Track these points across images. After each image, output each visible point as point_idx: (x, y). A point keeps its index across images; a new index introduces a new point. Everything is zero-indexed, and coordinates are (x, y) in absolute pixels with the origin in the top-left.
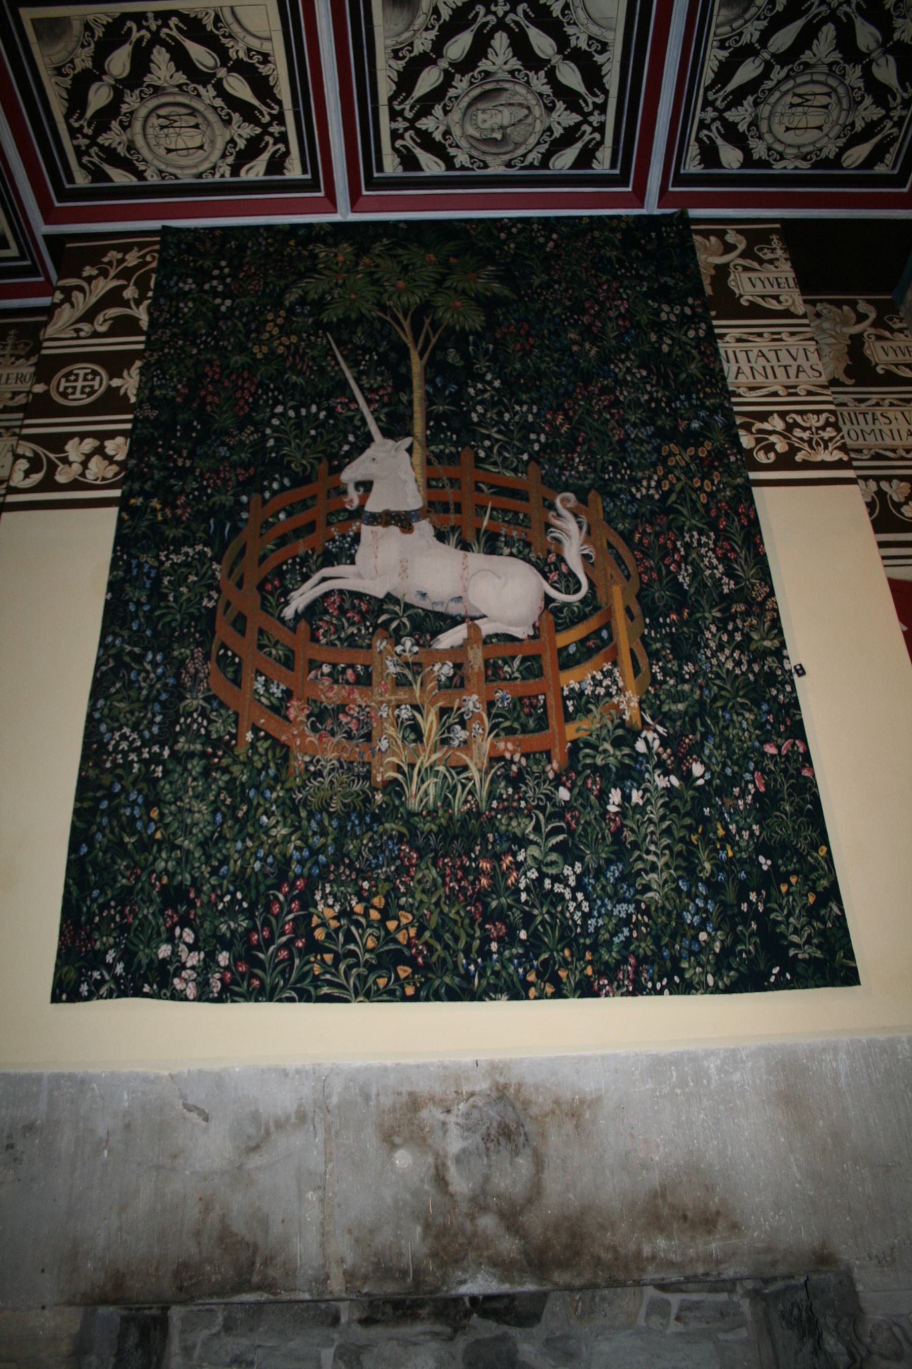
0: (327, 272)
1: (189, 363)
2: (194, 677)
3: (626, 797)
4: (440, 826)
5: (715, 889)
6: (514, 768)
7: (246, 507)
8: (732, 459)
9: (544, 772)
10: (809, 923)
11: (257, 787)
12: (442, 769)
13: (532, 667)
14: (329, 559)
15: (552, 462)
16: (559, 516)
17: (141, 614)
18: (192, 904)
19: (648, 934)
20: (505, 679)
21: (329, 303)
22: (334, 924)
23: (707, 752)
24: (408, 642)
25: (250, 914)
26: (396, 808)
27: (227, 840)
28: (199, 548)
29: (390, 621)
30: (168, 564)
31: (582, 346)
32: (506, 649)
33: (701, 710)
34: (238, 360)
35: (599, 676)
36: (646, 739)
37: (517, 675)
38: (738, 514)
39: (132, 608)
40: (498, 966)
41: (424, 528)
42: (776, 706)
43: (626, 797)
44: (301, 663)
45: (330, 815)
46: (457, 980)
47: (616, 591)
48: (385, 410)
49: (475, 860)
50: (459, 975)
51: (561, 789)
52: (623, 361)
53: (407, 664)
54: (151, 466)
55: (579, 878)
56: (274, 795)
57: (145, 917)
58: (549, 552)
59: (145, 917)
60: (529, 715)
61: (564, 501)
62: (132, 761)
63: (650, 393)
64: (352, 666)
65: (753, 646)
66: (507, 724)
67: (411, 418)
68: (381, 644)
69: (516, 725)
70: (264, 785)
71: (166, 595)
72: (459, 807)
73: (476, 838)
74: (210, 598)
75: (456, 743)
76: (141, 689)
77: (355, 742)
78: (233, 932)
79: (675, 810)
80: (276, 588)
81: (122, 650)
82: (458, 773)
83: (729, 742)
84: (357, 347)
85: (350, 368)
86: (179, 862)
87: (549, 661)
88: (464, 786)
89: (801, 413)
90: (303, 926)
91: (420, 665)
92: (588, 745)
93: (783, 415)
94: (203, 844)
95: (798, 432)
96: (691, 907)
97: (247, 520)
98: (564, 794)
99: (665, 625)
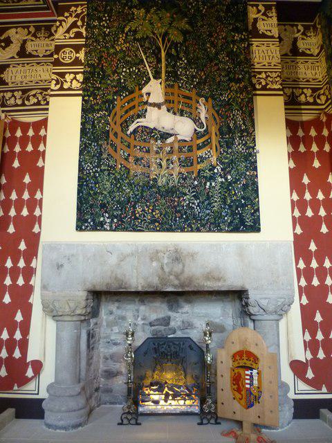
1: (98, 51)
3: (211, 184)
5: (230, 206)
7: (116, 100)
11: (122, 179)
14: (139, 116)
15: (199, 88)
24: (159, 141)
25: (121, 210)
29: (154, 135)
32: (184, 144)
34: (112, 51)
41: (164, 108)
43: (211, 184)
44: (132, 146)
47: (214, 127)
61: (202, 100)
68: (152, 142)
72: (171, 185)
80: (125, 125)
87: (195, 148)
89: (271, 72)
93: (266, 72)
95: (269, 79)
98: (196, 183)
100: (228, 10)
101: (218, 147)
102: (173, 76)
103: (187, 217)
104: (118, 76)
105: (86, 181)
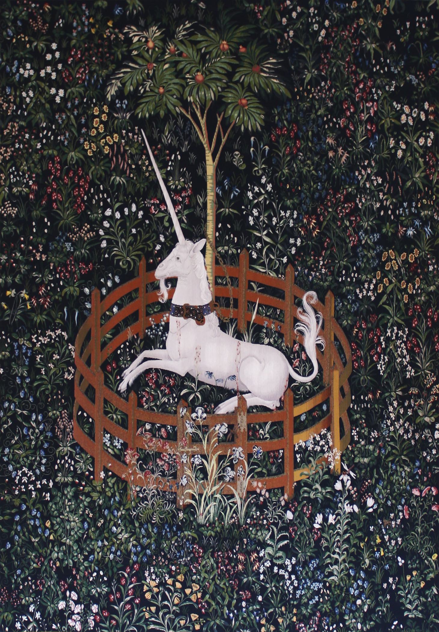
0: (140, 61)
3: (325, 519)
4: (216, 532)
6: (262, 499)
7: (88, 298)
8: (431, 268)
9: (279, 501)
10: (418, 598)
11: (109, 508)
12: (218, 496)
17: (25, 386)
18: (74, 578)
19: (329, 600)
20: (260, 439)
21: (142, 97)
22: (156, 590)
23: (377, 491)
24: (200, 410)
25: (108, 584)
26: (191, 522)
27: (92, 540)
28: (59, 332)
29: (188, 394)
30: (38, 345)
31: (336, 151)
33: (378, 463)
35: (318, 438)
36: (342, 481)
37: (267, 436)
38: (426, 317)
39: (18, 381)
40: (245, 615)
41: (212, 319)
42: (424, 464)
43: (325, 519)
44: (132, 423)
45: (153, 525)
46: (223, 621)
47: (336, 374)
48: (186, 212)
49: (235, 554)
50: (224, 619)
51: (288, 512)
52: (365, 168)
54: (17, 261)
55: (294, 566)
56: (120, 513)
57: (49, 586)
58: (295, 343)
59: (49, 586)
60: (273, 464)
62: (31, 490)
63: (381, 201)
64: (164, 426)
65: (418, 421)
66: (259, 470)
67: (206, 221)
68: (183, 411)
69: (264, 471)
70: (113, 507)
71: (40, 370)
72: (228, 520)
73: (237, 540)
74: (69, 372)
75: (227, 479)
76: (31, 440)
77: (167, 478)
78: (100, 594)
79: (353, 527)
80: (114, 368)
81: (16, 412)
82: (228, 499)
83: (392, 484)
84: (165, 147)
85: (160, 169)
86: (65, 553)
87: (288, 426)
88: (231, 507)
90: (139, 591)
91: (207, 426)
92: (306, 484)
94: (77, 542)
96: (355, 585)
97: (90, 309)
98: (289, 515)
99: (364, 401)
100: (387, 34)
102: (234, 231)
103: (266, 599)
104: (91, 230)
105: (21, 513)
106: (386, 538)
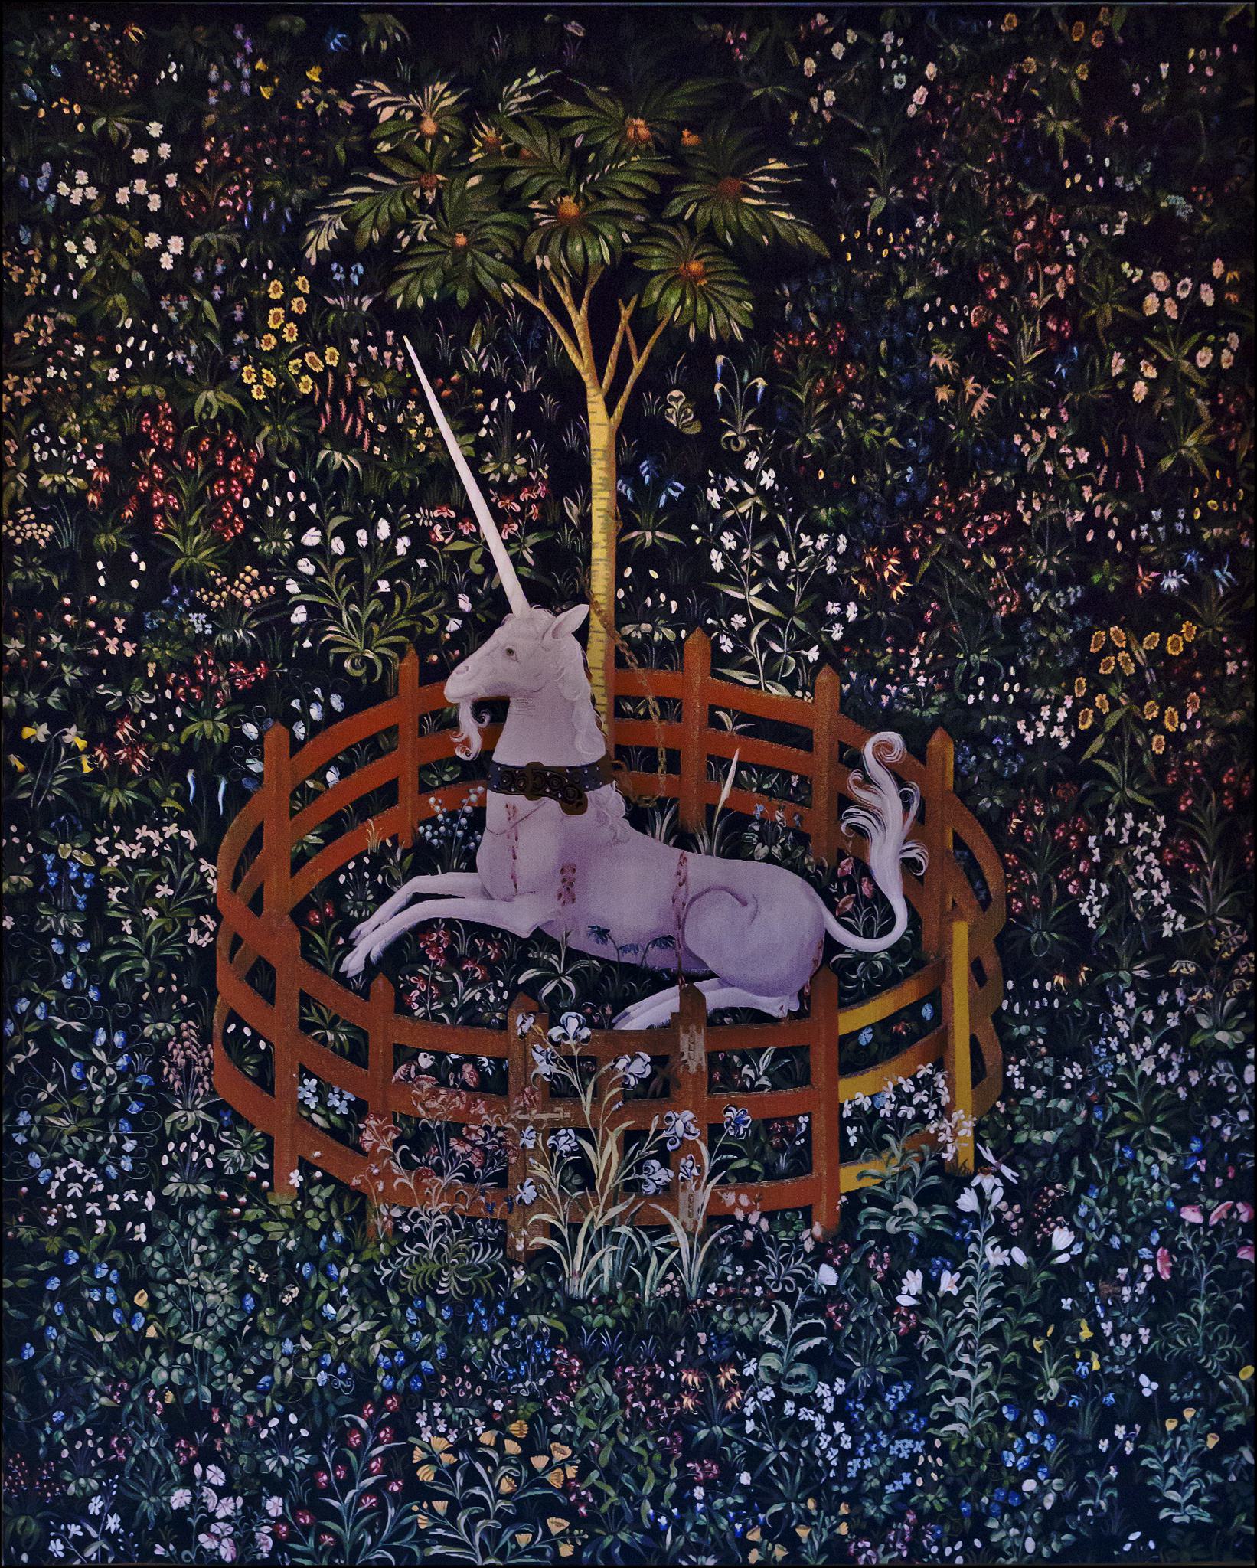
2: (186, 1072)
3: (931, 1284)
4: (619, 1318)
6: (749, 1235)
9: (798, 1241)
10: (1201, 1475)
11: (315, 1260)
12: (625, 1230)
13: (792, 1069)
16: (867, 781)
17: (75, 960)
18: (216, 1431)
19: (940, 1482)
20: (743, 1088)
22: (448, 1459)
25: (313, 1446)
26: (549, 1293)
27: (266, 1338)
35: (908, 1087)
36: (979, 1190)
37: (763, 1081)
40: (703, 1520)
41: (608, 798)
43: (931, 1284)
45: (439, 1301)
46: (638, 1537)
47: (960, 931)
49: (675, 1370)
50: (643, 1531)
51: (824, 1267)
53: (570, 1060)
55: (839, 1401)
56: (345, 1272)
57: (145, 1452)
58: (842, 855)
59: (145, 1452)
60: (781, 1149)
62: (93, 1216)
64: (473, 1059)
66: (743, 1163)
68: (524, 1023)
69: (756, 1167)
70: (327, 1257)
72: (651, 1288)
73: (678, 1338)
74: (202, 929)
75: (651, 1189)
76: (93, 1094)
77: (478, 1186)
78: (287, 1471)
79: (1014, 1301)
80: (328, 917)
81: (52, 1025)
82: (653, 1238)
83: (1123, 1194)
86: (189, 1370)
87: (822, 1060)
88: (661, 1258)
90: (399, 1463)
91: (594, 1060)
92: (875, 1199)
94: (224, 1342)
96: (1017, 1444)
98: (827, 1276)
99: (1042, 993)
101: (992, 1053)
105: (64, 1271)
106: (1107, 1327)
